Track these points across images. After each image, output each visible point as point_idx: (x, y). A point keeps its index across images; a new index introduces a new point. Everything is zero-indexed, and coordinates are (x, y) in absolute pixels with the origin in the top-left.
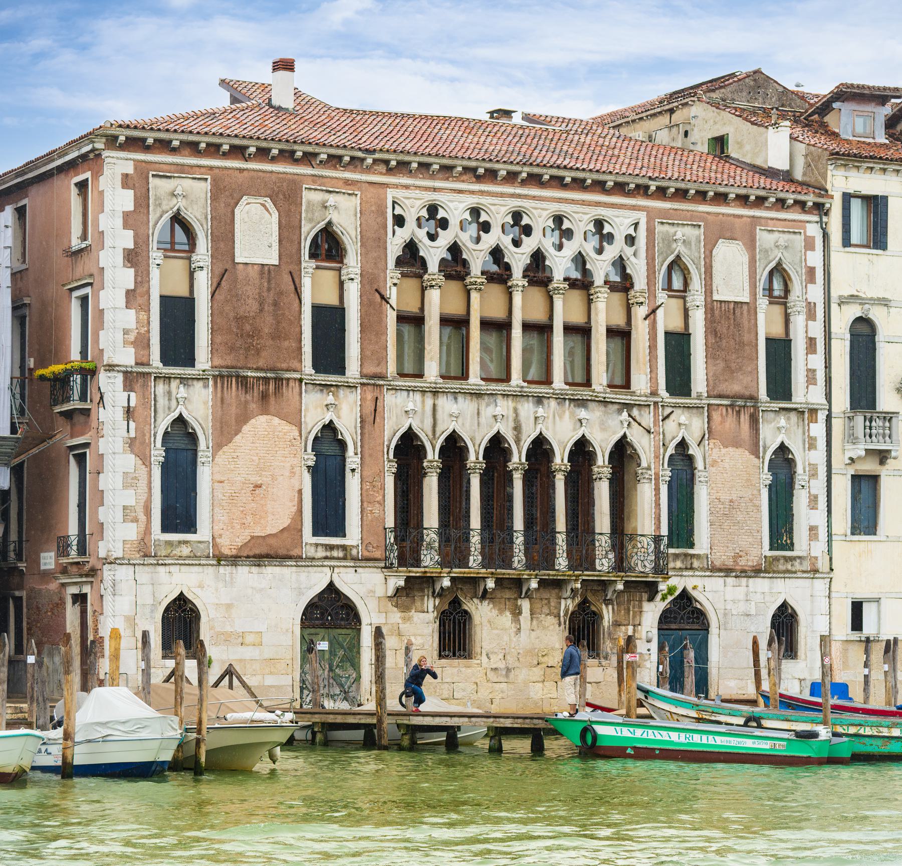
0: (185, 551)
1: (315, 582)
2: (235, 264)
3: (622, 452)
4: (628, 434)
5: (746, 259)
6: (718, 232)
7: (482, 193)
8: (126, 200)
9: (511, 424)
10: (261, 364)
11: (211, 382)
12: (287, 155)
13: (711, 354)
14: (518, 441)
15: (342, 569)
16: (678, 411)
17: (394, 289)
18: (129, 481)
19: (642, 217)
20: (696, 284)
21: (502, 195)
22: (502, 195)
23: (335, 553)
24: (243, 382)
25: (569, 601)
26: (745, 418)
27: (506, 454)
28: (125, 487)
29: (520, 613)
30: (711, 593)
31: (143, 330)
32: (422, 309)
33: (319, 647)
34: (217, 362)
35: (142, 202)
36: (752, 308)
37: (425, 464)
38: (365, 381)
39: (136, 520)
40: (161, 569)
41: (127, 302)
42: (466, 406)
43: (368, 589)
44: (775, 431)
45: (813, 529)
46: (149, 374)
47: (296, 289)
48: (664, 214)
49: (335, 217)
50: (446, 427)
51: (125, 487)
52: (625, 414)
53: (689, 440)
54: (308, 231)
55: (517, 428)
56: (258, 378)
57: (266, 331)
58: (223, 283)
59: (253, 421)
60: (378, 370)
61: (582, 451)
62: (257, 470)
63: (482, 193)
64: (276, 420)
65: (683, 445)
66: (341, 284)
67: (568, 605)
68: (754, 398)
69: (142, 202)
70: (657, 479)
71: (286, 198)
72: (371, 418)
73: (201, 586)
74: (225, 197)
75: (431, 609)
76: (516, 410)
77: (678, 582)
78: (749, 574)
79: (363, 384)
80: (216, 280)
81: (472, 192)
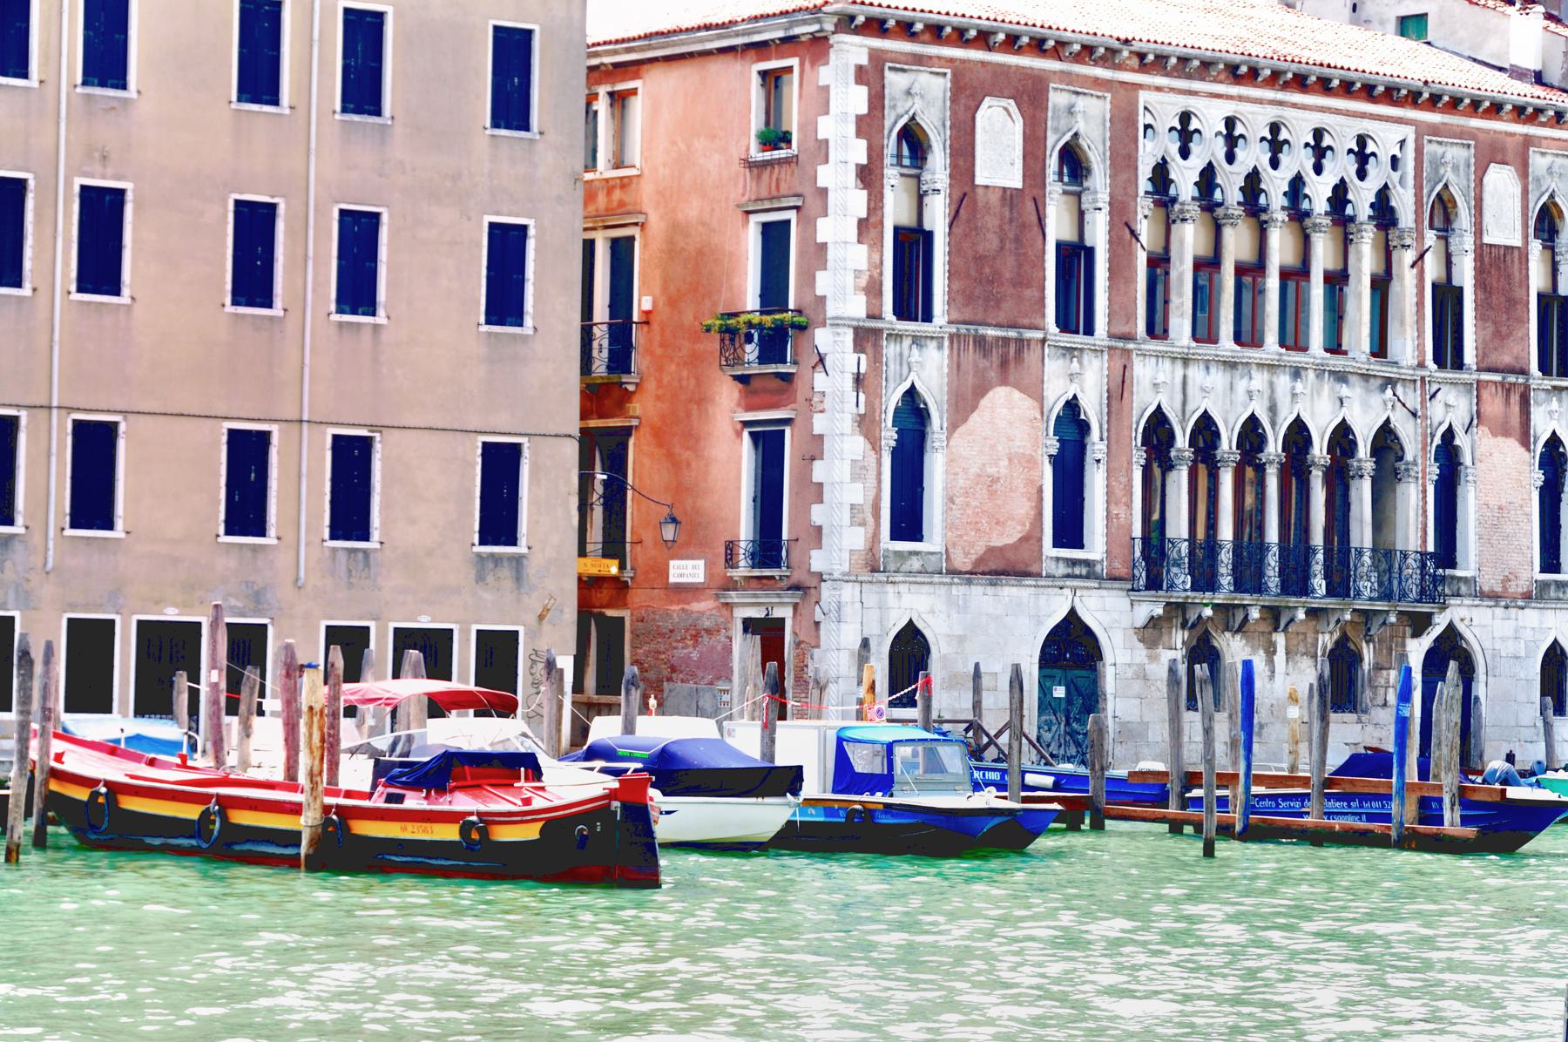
0: (915, 564)
1: (1055, 609)
2: (974, 186)
3: (1386, 440)
4: (1392, 419)
5: (1518, 190)
6: (1490, 153)
7: (1240, 98)
8: (857, 99)
9: (1266, 403)
10: (1002, 318)
11: (946, 343)
12: (1038, 45)
13: (1480, 317)
14: (1273, 424)
15: (1085, 592)
16: (1445, 388)
17: (1145, 222)
18: (858, 472)
19: (1409, 133)
20: (1464, 219)
21: (1260, 101)
22: (1260, 101)
23: (1077, 571)
24: (981, 341)
25: (1327, 636)
26: (1515, 398)
27: (1262, 441)
28: (853, 480)
29: (1274, 652)
31: (876, 273)
32: (1167, 248)
33: (1056, 695)
34: (955, 316)
35: (877, 100)
36: (1523, 254)
37: (1173, 454)
38: (1113, 343)
39: (863, 524)
40: (890, 588)
41: (860, 234)
42: (1218, 378)
43: (1113, 616)
46: (880, 331)
47: (1040, 219)
48: (1435, 130)
49: (1080, 126)
51: (853, 480)
52: (1389, 392)
54: (1054, 143)
55: (1273, 409)
56: (997, 338)
57: (1008, 276)
58: (962, 211)
59: (991, 394)
60: (1125, 329)
61: (1343, 437)
62: (990, 457)
63: (1240, 98)
64: (1016, 394)
65: (1449, 434)
66: (1081, 214)
67: (1327, 640)
68: (1524, 372)
69: (877, 100)
70: (1424, 478)
71: (1030, 97)
72: (1119, 390)
73: (932, 612)
74: (967, 94)
75: (1179, 645)
76: (1271, 384)
78: (1520, 603)
79: (1110, 348)
80: (954, 207)
81: (1230, 97)
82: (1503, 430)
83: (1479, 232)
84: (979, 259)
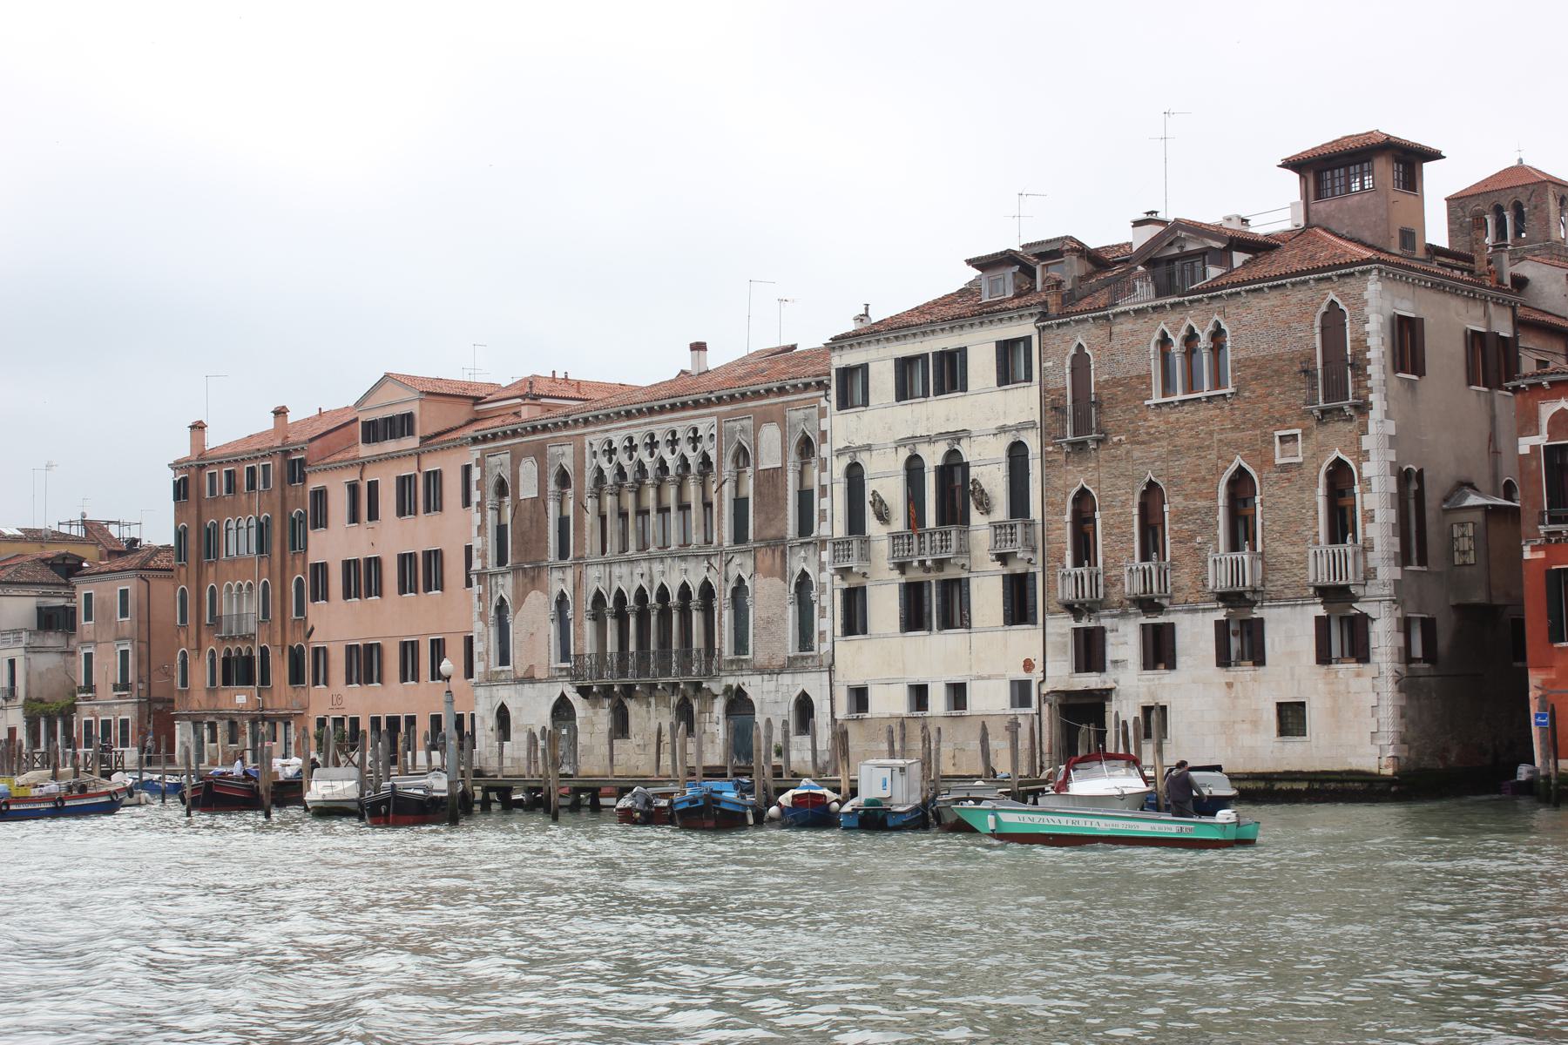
0: (503, 676)
3: (707, 590)
6: (764, 418)
19: (715, 419)
26: (778, 554)
30: (755, 687)
44: (796, 564)
45: (822, 634)
48: (728, 414)
50: (616, 584)
53: (744, 576)
55: (651, 581)
61: (685, 590)
67: (675, 700)
77: (733, 681)
82: (770, 573)
83: (756, 464)
84: (523, 534)
